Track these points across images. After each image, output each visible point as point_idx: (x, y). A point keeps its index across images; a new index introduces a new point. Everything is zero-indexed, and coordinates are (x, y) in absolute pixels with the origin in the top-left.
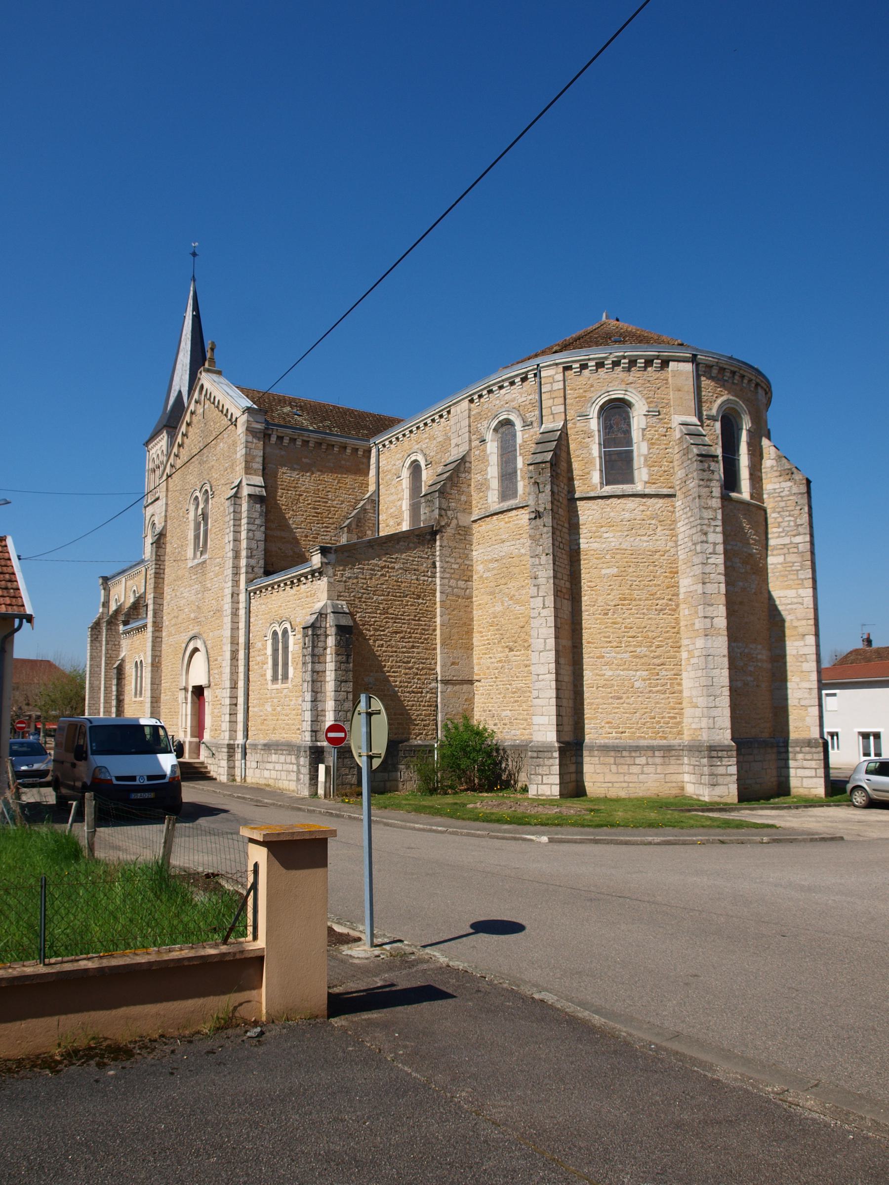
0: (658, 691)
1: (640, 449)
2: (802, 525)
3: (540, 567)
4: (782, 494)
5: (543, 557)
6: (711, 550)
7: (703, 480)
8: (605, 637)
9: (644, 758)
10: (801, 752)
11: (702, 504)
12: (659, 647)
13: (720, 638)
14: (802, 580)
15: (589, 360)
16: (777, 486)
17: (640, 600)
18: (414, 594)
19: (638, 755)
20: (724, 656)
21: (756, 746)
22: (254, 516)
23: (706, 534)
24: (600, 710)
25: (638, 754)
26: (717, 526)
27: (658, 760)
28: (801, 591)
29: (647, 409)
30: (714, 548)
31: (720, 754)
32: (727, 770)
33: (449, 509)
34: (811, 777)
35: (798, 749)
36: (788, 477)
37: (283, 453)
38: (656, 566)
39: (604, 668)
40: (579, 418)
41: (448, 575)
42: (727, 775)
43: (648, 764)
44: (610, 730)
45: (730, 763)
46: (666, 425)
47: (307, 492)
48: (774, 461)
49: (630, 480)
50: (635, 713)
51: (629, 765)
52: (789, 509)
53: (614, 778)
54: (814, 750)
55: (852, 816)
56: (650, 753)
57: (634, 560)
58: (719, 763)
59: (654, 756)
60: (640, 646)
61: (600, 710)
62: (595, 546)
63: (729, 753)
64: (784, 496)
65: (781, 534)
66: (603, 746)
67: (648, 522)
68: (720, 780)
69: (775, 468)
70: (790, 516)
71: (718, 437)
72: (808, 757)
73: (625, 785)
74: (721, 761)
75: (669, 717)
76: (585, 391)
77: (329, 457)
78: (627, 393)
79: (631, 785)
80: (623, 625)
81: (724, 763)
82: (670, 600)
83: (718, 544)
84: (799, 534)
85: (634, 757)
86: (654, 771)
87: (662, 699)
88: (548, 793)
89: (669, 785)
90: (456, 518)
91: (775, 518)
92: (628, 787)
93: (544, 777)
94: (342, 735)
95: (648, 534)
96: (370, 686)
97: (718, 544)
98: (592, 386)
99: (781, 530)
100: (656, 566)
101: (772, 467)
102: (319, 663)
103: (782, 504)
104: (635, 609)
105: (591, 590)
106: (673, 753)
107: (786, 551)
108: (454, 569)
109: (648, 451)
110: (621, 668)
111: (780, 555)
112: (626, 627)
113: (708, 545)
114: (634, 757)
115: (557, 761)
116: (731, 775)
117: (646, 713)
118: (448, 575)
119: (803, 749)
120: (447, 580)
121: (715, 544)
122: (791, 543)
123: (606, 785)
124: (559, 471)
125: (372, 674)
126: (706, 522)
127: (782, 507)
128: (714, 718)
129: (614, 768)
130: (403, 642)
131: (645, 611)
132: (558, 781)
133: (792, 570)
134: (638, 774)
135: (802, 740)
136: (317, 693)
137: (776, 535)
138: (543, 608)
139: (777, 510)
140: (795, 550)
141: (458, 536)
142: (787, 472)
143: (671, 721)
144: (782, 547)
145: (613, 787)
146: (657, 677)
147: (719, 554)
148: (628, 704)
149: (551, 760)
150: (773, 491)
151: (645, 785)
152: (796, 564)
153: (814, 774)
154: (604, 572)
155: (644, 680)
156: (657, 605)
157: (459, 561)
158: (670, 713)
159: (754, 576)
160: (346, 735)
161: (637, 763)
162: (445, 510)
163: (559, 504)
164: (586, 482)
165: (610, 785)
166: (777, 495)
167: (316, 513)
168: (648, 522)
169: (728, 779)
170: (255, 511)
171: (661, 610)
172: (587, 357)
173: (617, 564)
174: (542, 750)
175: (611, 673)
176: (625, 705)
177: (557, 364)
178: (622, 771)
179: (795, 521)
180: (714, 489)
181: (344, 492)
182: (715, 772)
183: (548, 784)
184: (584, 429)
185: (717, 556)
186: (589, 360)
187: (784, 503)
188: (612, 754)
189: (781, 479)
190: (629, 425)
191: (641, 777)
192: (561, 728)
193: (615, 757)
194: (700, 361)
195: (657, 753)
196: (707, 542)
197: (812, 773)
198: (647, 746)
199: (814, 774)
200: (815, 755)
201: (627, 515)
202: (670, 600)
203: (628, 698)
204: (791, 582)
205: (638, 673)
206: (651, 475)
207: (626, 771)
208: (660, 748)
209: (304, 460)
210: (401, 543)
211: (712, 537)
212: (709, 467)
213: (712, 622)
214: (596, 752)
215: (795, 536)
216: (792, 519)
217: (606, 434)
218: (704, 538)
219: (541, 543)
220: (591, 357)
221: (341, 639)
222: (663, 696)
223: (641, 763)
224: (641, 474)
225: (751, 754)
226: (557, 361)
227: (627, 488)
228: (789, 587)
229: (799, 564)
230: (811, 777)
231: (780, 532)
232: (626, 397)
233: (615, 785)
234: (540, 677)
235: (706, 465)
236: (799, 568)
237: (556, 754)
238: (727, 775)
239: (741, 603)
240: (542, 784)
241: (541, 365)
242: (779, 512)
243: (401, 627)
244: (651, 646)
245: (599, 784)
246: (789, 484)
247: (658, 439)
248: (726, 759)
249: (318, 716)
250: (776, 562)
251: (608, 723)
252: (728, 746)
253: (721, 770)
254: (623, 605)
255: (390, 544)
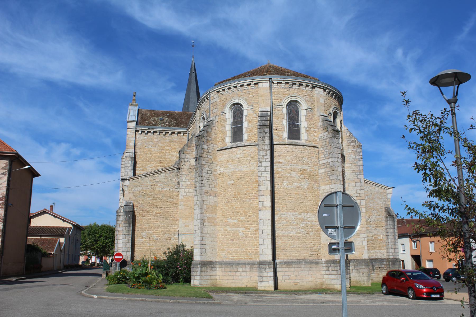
0: (249, 237)
1: (245, 124)
2: (331, 153)
3: (197, 182)
4: (324, 139)
5: (198, 178)
6: (264, 170)
7: (260, 137)
8: (228, 213)
9: (242, 268)
10: (330, 266)
11: (260, 149)
12: (250, 216)
13: (267, 211)
14: (331, 180)
15: (225, 87)
16: (322, 135)
17: (242, 194)
18: (168, 196)
19: (239, 267)
20: (269, 220)
21: (303, 263)
22: (128, 166)
23: (261, 162)
24: (226, 246)
25: (239, 267)
26: (267, 158)
27: (248, 270)
28: (331, 185)
29: (247, 106)
30: (265, 169)
31: (264, 266)
32: (268, 274)
33: (186, 158)
34: (334, 279)
35: (329, 265)
36: (326, 130)
37: (145, 138)
38: (250, 178)
39: (227, 227)
40: (222, 114)
41: (184, 187)
42: (268, 276)
43: (243, 271)
44: (229, 256)
45: (270, 271)
46: (256, 113)
47: (156, 153)
48: (321, 123)
49: (242, 140)
50: (239, 247)
51: (235, 272)
52: (326, 145)
53: (228, 278)
54: (335, 265)
55: (322, 298)
56: (244, 266)
57: (240, 176)
58: (264, 271)
59: (246, 268)
60: (242, 216)
61: (226, 246)
62: (226, 171)
63: (269, 266)
64: (324, 140)
65: (324, 158)
66: (226, 263)
67: (247, 158)
68: (264, 279)
69: (322, 126)
70: (327, 149)
71: (284, 115)
72: (333, 269)
73: (234, 281)
74: (265, 270)
75: (254, 249)
76: (224, 101)
77: (167, 137)
78: (239, 100)
79: (236, 281)
80: (235, 207)
81: (266, 271)
82: (256, 194)
83: (267, 166)
84: (330, 158)
85: (238, 268)
86: (246, 275)
87: (251, 241)
88: (196, 284)
89: (253, 281)
90: (190, 162)
91: (321, 150)
92: (235, 282)
93: (195, 277)
94: (121, 257)
95: (247, 164)
96: (144, 237)
97: (267, 166)
98: (227, 99)
99: (324, 156)
100: (250, 178)
101: (321, 125)
102: (119, 227)
103: (324, 143)
104: (240, 199)
105: (224, 191)
106: (255, 266)
107: (325, 166)
108: (187, 184)
109: (248, 126)
110: (234, 226)
111: (323, 168)
112: (236, 208)
113: (262, 167)
114: (238, 268)
115: (199, 269)
116: (270, 277)
117: (244, 247)
118: (184, 187)
119: (331, 265)
120: (184, 189)
121: (266, 167)
122: (328, 162)
123: (227, 281)
124: (210, 139)
125: (145, 231)
126: (262, 157)
127: (324, 145)
128: (263, 249)
129: (229, 273)
130: (161, 217)
131: (244, 200)
132: (199, 279)
133: (328, 176)
134: (239, 276)
135: (331, 260)
136: (118, 240)
137: (322, 159)
138: (198, 201)
139: (322, 146)
140: (329, 166)
141: (190, 170)
142: (326, 127)
143: (255, 251)
144: (324, 164)
145: (229, 282)
146: (249, 230)
147: (268, 171)
148: (236, 243)
149: (197, 269)
150: (321, 137)
151: (242, 281)
152: (329, 173)
153: (335, 278)
154: (229, 182)
155: (243, 232)
156: (249, 197)
157: (190, 180)
158: (254, 247)
159: (306, 180)
160: (122, 257)
161: (238, 271)
162: (184, 159)
163: (209, 154)
164: (223, 142)
165: (228, 281)
166: (322, 139)
167: (160, 162)
168: (247, 158)
169: (269, 278)
170: (129, 164)
171: (252, 199)
172: (224, 86)
173: (233, 179)
174: (195, 264)
175: (229, 229)
176: (235, 244)
177: (214, 91)
178: (233, 275)
179: (329, 151)
180: (266, 141)
181: (174, 152)
182: (262, 276)
183: (196, 280)
184: (223, 118)
185: (267, 172)
186: (225, 87)
187: (325, 143)
188: (229, 266)
189: (324, 131)
190: (242, 115)
191: (241, 278)
192: (203, 254)
193: (230, 268)
194: (273, 81)
195: (247, 266)
196: (261, 166)
197: (334, 277)
198: (243, 263)
199: (335, 278)
200: (335, 268)
201: (238, 156)
202: (256, 194)
203: (236, 240)
204: (327, 182)
205: (241, 229)
206: (248, 136)
207: (234, 275)
208: (249, 264)
209: (154, 140)
210: (161, 175)
211: (264, 164)
212: (264, 131)
213: (263, 204)
214: (223, 266)
215: (328, 159)
216: (328, 150)
217: (234, 119)
218: (261, 165)
219: (197, 172)
220: (225, 86)
221: (126, 217)
222: (251, 239)
223: (240, 271)
224: (245, 136)
225: (300, 267)
226: (214, 90)
227: (239, 144)
228: (326, 184)
229: (330, 172)
230: (334, 279)
231: (323, 157)
232: (239, 102)
233: (230, 281)
234: (196, 231)
235: (263, 130)
236: (330, 174)
237: (199, 266)
238: (268, 276)
239: (296, 194)
240: (195, 280)
241: (210, 92)
242: (323, 148)
243: (160, 211)
244: (247, 216)
245: (224, 281)
246: (326, 133)
247: (252, 120)
248: (268, 269)
249: (118, 250)
250: (322, 172)
251: (229, 252)
252: (269, 263)
253: (265, 274)
254: (235, 197)
255: (155, 175)
